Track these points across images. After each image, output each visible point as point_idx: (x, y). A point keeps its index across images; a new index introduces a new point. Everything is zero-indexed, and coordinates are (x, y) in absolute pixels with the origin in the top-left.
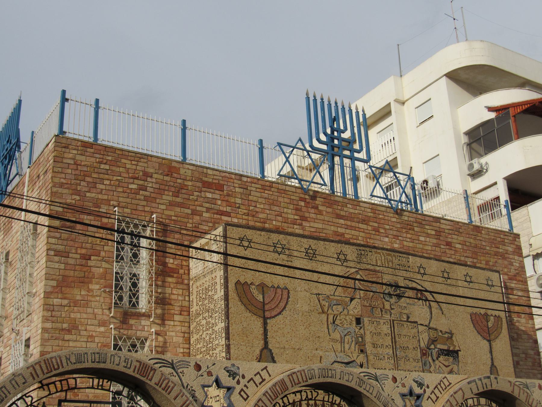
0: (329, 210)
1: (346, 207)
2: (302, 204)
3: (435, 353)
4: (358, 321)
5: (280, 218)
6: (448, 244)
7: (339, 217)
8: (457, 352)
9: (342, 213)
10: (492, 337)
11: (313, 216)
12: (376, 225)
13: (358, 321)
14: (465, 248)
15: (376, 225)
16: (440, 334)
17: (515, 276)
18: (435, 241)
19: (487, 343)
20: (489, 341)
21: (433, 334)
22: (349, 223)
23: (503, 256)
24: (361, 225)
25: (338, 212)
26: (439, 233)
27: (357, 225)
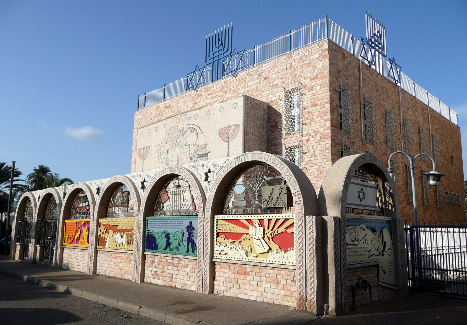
0: (206, 93)
1: (213, 87)
2: (196, 96)
3: (195, 157)
4: (168, 152)
5: (187, 108)
6: (265, 79)
7: (209, 95)
8: (207, 154)
9: (211, 92)
10: (230, 139)
11: (199, 100)
12: (226, 89)
13: (168, 152)
14: (278, 74)
15: (226, 89)
16: (200, 147)
17: (317, 75)
18: (257, 81)
19: (227, 143)
20: (228, 142)
21: (196, 148)
22: (213, 96)
23: (309, 65)
24: (219, 94)
25: (209, 92)
26: (260, 75)
27: (217, 94)
